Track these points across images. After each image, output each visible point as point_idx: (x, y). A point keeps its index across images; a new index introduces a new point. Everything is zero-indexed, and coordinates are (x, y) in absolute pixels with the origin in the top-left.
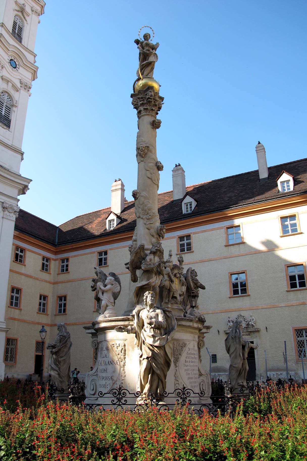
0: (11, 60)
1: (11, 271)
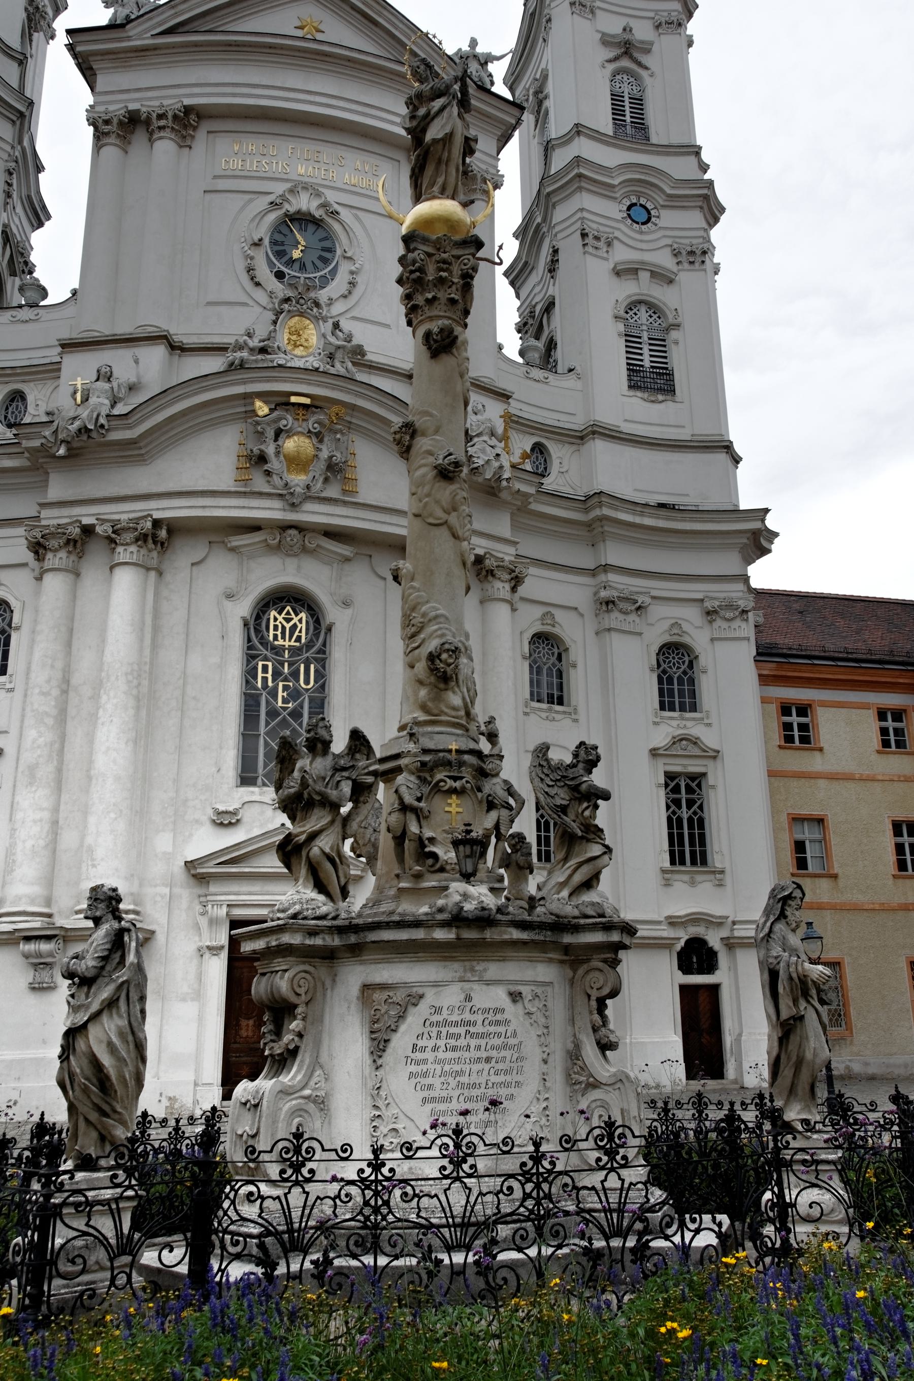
0: (629, 208)
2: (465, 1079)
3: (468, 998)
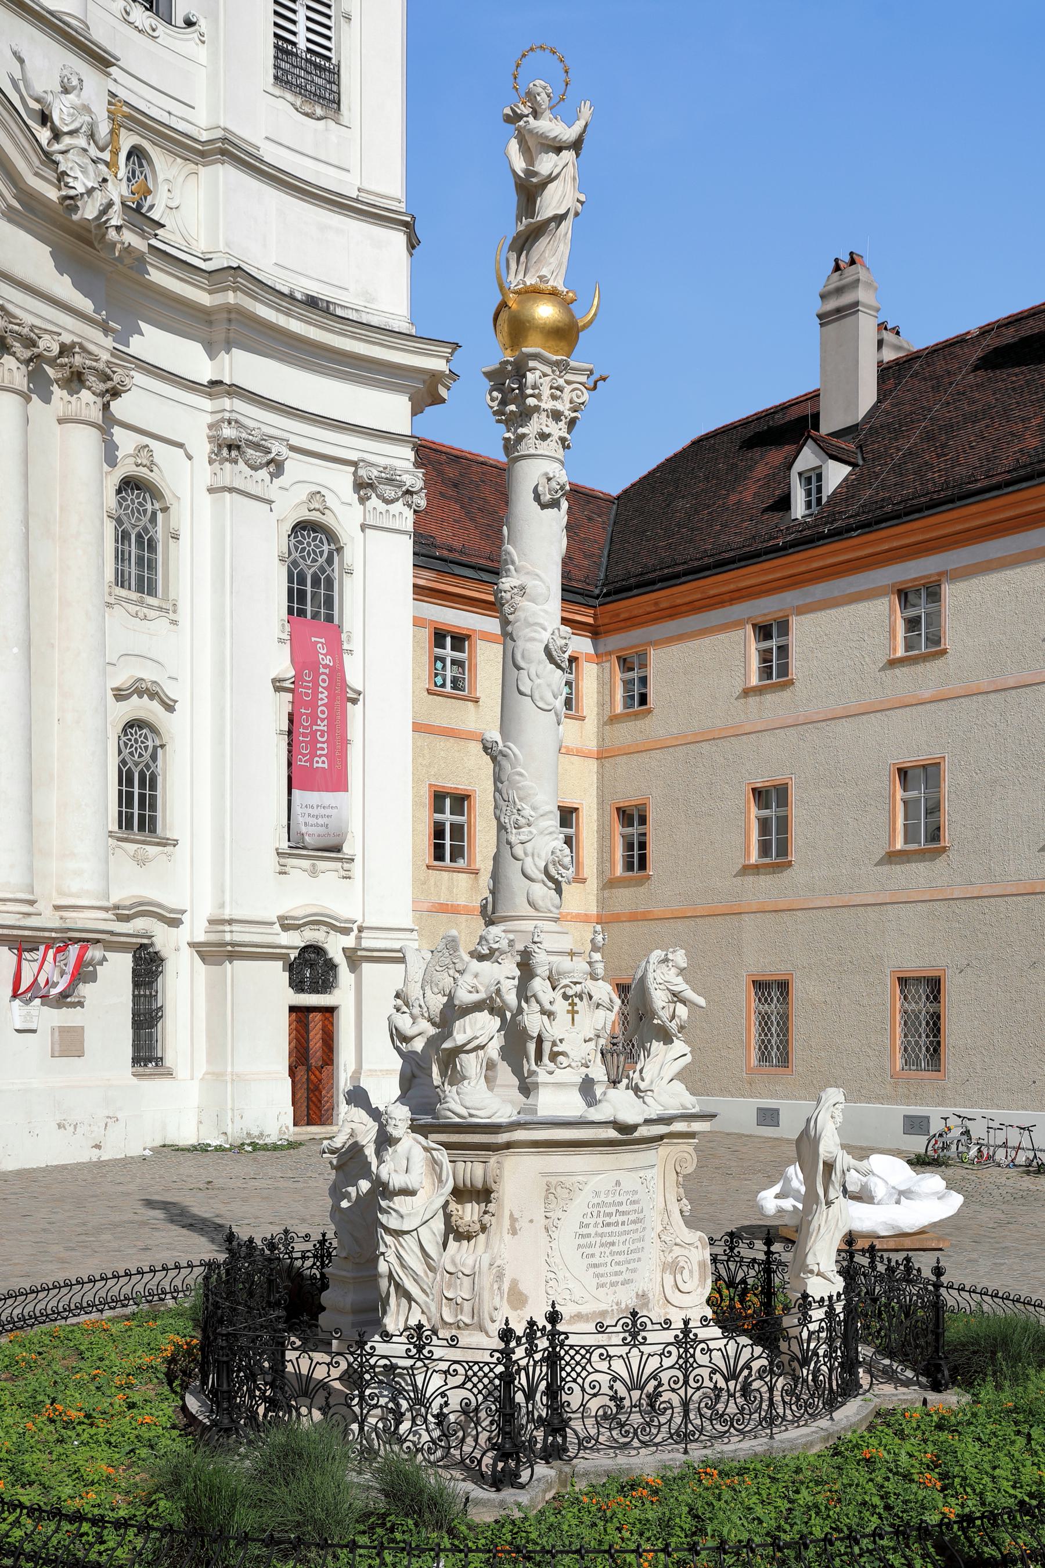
1: (418, 728)
2: (615, 1249)
3: (618, 1183)
